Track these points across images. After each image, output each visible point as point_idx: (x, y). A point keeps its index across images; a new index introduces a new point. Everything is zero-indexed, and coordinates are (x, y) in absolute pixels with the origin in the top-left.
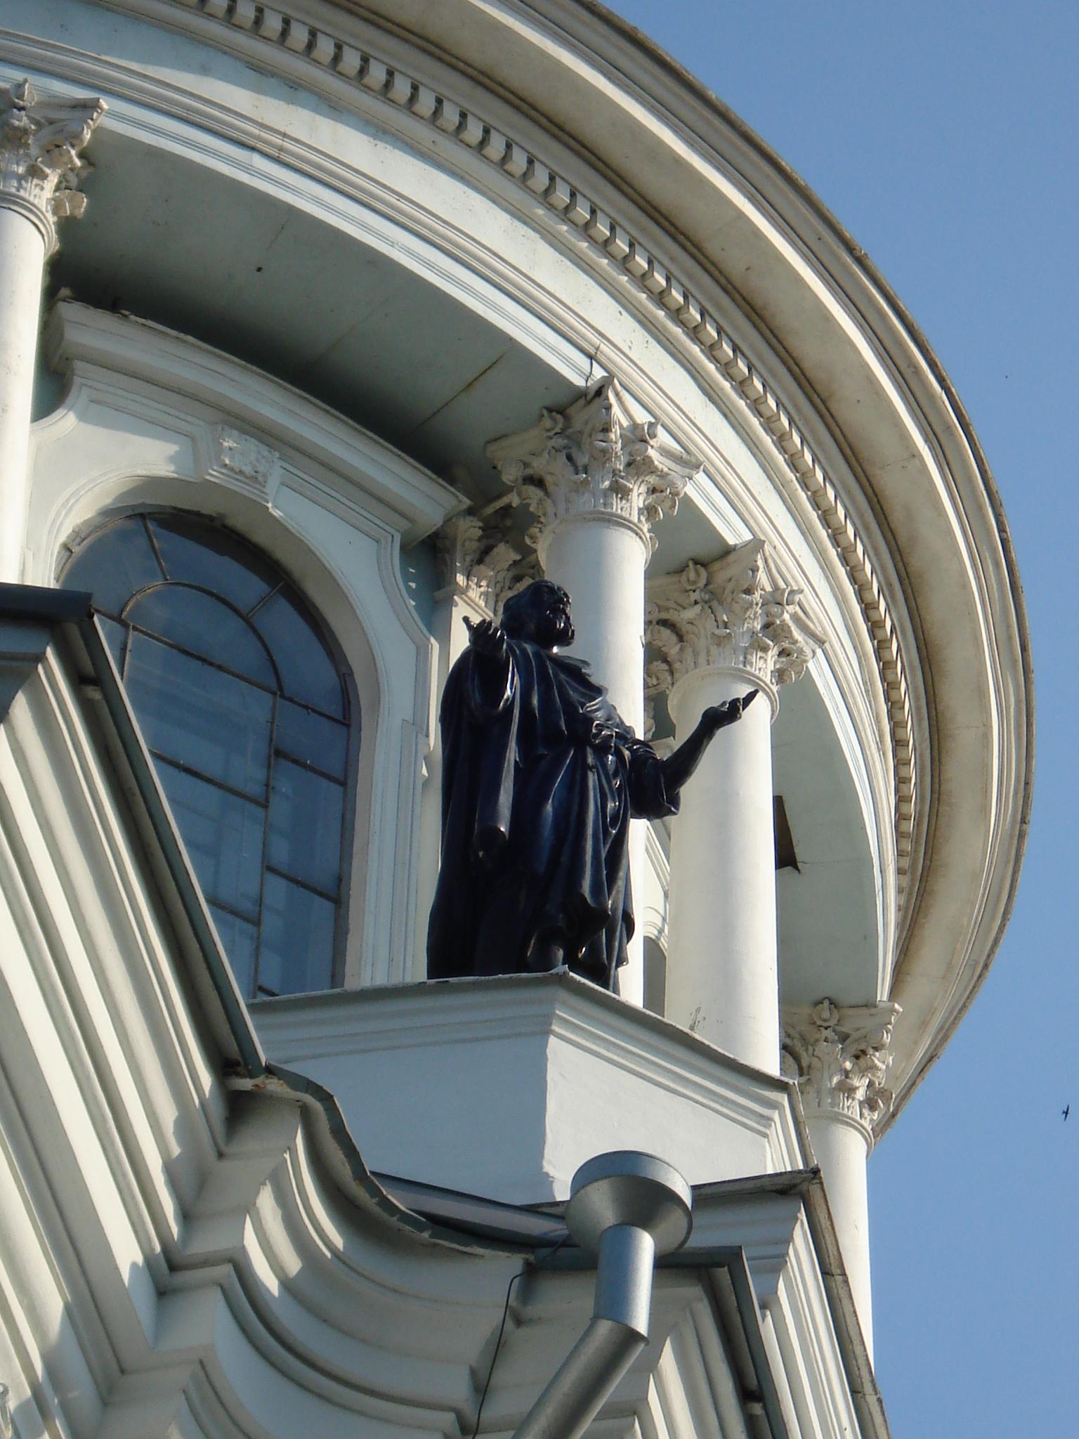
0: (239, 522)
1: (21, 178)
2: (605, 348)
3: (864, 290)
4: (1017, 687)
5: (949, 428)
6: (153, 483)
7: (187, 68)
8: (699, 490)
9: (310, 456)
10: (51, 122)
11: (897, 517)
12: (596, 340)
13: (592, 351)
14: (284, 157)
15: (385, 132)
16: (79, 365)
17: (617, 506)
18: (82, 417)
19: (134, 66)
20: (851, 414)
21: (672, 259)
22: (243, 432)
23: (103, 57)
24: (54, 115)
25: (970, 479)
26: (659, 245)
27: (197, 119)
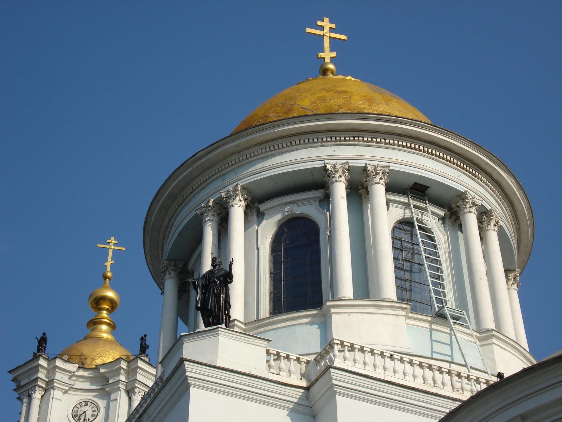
0: (295, 216)
1: (233, 201)
2: (325, 157)
3: (364, 116)
4: (452, 135)
5: (397, 119)
6: (279, 221)
7: (252, 166)
8: (352, 163)
9: (298, 201)
10: (235, 190)
11: (404, 134)
12: (323, 157)
13: (324, 159)
14: (266, 170)
15: (282, 153)
16: (264, 212)
17: (334, 179)
18: (266, 220)
19: (246, 172)
20: (381, 129)
21: (335, 134)
22: (288, 205)
23: (242, 174)
24: (235, 189)
25: (409, 121)
26: (330, 134)
27: (253, 174)
